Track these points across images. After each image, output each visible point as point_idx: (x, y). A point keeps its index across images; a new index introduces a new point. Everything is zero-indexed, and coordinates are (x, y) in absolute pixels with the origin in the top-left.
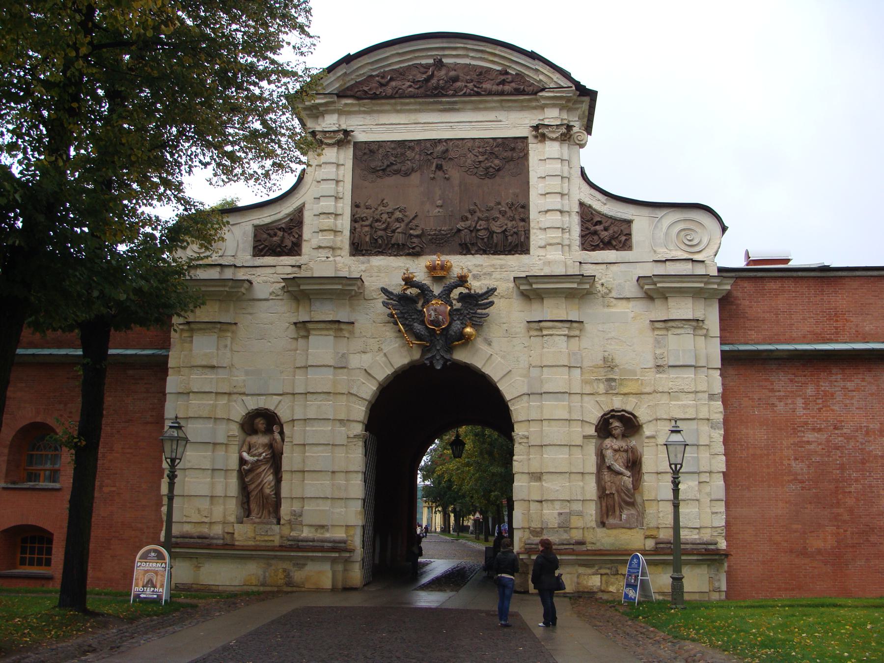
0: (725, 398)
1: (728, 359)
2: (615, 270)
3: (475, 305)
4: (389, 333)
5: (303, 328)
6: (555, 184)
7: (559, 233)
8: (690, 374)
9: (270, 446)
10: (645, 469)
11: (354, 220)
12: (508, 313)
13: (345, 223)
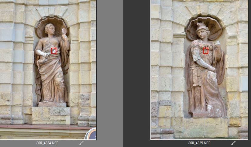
9: (59, 46)
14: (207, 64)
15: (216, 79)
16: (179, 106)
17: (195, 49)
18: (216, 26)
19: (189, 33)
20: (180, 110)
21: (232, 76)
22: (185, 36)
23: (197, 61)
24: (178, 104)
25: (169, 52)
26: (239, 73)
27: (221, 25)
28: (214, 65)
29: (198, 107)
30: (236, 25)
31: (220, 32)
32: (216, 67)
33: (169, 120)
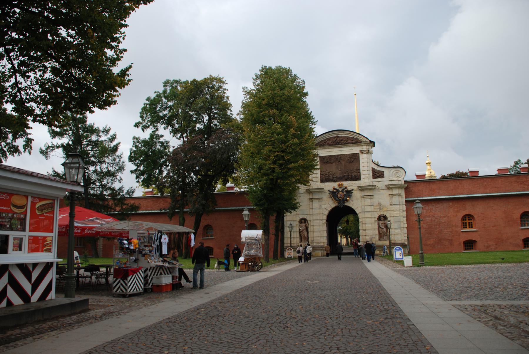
0: (407, 211)
1: (406, 201)
2: (380, 183)
3: (349, 193)
4: (330, 200)
5: (311, 200)
6: (366, 164)
7: (367, 176)
8: (398, 206)
9: (306, 226)
11: (321, 175)
12: (357, 194)
13: (319, 175)
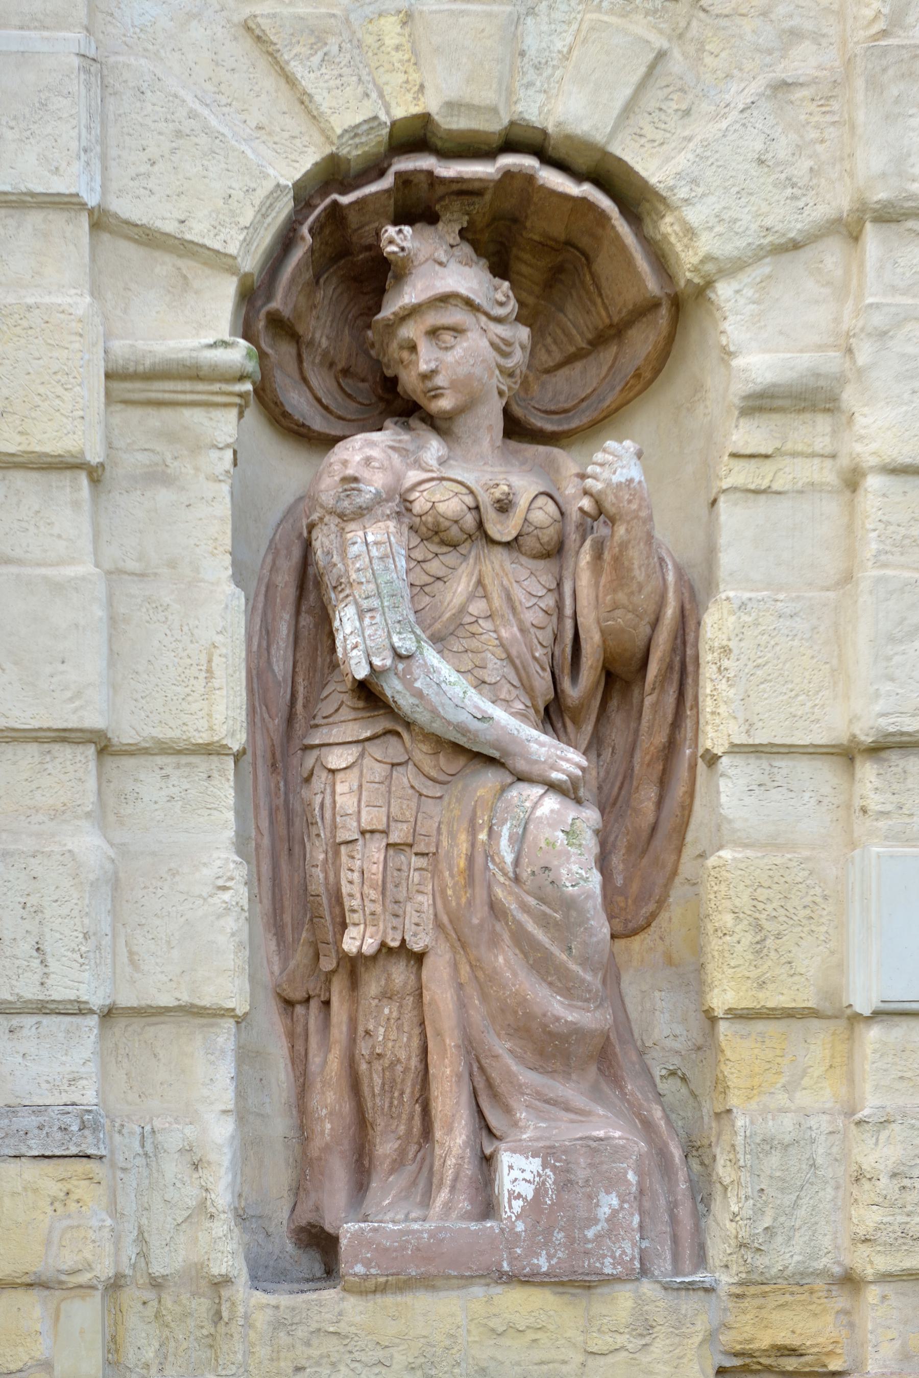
10: (721, 717)
14: (499, 714)
15: (596, 878)
16: (196, 1166)
17: (355, 533)
18: (603, 265)
19: (287, 350)
20: (203, 1210)
21: (773, 844)
22: (248, 387)
23: (384, 672)
24: (173, 1141)
25: (70, 571)
26: (849, 806)
27: (661, 259)
28: (576, 722)
29: (392, 1171)
30: (831, 255)
31: (642, 342)
32: (595, 746)
33: (85, 1314)
